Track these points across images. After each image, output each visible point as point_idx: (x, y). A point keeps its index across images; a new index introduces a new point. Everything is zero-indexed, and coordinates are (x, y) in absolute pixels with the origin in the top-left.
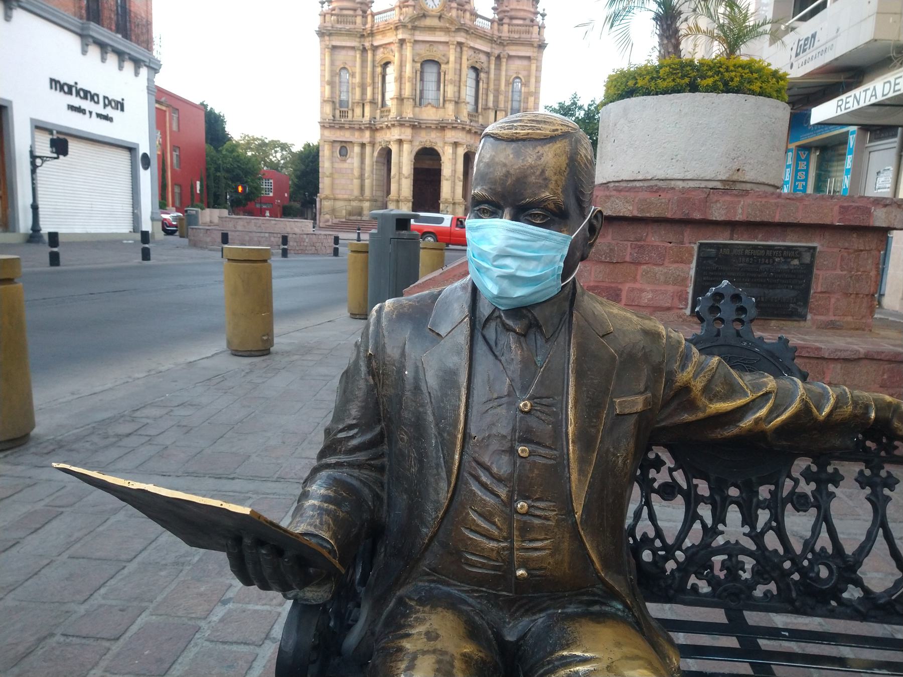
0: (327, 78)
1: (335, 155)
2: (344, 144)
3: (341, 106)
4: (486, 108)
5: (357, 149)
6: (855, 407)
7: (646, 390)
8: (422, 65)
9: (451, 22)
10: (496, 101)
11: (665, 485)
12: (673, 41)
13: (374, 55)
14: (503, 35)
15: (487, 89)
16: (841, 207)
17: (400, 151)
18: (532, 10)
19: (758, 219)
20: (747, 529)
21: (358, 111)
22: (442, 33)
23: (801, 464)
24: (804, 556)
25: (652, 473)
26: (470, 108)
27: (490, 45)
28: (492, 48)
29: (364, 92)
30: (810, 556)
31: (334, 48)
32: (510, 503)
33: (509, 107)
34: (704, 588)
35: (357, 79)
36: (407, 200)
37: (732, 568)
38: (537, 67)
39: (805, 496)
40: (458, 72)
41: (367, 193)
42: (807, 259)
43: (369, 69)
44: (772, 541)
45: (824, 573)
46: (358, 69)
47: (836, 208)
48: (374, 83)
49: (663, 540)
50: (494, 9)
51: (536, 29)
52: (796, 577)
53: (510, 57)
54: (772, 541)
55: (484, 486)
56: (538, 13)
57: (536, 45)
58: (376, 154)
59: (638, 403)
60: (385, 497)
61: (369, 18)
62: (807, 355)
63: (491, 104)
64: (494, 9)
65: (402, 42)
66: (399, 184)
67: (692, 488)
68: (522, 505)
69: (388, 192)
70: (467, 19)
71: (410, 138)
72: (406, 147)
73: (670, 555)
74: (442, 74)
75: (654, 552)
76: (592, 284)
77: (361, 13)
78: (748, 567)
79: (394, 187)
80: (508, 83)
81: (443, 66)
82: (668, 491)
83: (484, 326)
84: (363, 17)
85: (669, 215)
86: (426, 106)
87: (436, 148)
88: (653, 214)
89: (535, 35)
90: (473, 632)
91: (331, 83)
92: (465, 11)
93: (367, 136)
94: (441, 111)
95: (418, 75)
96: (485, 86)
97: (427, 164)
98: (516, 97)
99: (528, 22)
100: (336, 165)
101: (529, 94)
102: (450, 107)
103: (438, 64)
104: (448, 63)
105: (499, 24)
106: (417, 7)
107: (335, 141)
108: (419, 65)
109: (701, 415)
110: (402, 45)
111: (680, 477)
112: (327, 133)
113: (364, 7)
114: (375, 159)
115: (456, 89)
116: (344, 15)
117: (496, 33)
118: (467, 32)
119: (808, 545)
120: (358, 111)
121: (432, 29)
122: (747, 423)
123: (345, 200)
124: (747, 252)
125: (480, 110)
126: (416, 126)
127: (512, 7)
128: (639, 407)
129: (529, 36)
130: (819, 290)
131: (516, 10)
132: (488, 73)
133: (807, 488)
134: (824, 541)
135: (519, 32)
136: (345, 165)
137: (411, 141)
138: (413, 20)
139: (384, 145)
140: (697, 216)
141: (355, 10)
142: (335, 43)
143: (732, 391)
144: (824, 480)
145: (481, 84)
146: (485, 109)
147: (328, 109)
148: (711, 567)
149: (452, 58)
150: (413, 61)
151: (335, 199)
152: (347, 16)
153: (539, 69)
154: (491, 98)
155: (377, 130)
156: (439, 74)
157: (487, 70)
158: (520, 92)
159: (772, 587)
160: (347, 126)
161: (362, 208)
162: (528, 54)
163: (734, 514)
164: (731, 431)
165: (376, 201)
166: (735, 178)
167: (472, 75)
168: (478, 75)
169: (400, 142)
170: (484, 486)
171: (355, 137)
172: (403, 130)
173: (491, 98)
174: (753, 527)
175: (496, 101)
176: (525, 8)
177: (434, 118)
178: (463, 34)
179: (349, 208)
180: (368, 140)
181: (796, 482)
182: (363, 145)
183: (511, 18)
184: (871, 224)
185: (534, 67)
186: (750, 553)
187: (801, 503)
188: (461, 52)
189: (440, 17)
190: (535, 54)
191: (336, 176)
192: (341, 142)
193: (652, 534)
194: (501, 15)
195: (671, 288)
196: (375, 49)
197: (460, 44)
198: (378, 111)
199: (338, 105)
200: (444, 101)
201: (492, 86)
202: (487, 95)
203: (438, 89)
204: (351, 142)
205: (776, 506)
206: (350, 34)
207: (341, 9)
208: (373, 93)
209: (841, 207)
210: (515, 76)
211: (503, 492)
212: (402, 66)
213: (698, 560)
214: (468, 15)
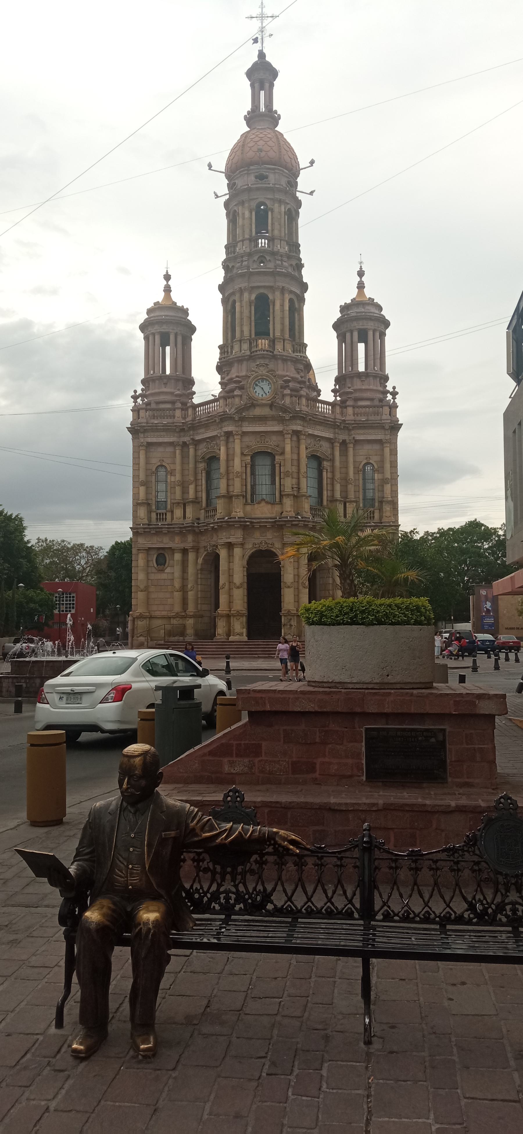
0: (142, 477)
1: (151, 564)
2: (161, 552)
3: (158, 508)
4: (333, 500)
6: (259, 833)
7: (177, 830)
8: (252, 457)
9: (284, 409)
10: (345, 491)
11: (205, 868)
12: (348, 581)
13: (196, 450)
14: (348, 418)
15: (333, 479)
16: (455, 701)
17: (230, 556)
18: (381, 389)
19: (399, 711)
20: (232, 884)
21: (178, 513)
22: (275, 423)
23: (255, 857)
24: (253, 893)
25: (201, 863)
26: (313, 501)
27: (332, 430)
28: (335, 433)
29: (185, 491)
30: (255, 892)
31: (149, 445)
32: (127, 866)
33: (361, 497)
34: (217, 907)
35: (178, 477)
36: (242, 615)
37: (227, 898)
38: (391, 450)
39: (253, 870)
40: (295, 463)
41: (191, 608)
42: (440, 738)
43: (191, 465)
44: (241, 888)
45: (259, 898)
46: (178, 467)
47: (452, 702)
48: (196, 480)
49: (203, 890)
50: (333, 391)
51: (386, 410)
52: (250, 901)
53: (356, 442)
54: (241, 888)
55: (120, 861)
56: (388, 392)
57: (387, 427)
58: (200, 561)
59: (173, 834)
60: (95, 871)
61: (190, 411)
62: (417, 809)
63: (338, 495)
64: (333, 391)
66: (230, 596)
67: (215, 868)
68: (130, 866)
69: (217, 606)
70: (303, 407)
71: (241, 540)
72: (237, 551)
73: (205, 895)
74: (277, 466)
75: (199, 894)
76: (294, 759)
77: (180, 405)
78: (233, 899)
79: (223, 599)
80: (357, 471)
81: (277, 457)
82: (206, 870)
83: (124, 811)
84: (182, 410)
85: (339, 710)
86: (259, 503)
88: (328, 709)
89: (385, 417)
90: (114, 903)
91: (146, 484)
92: (300, 397)
94: (277, 508)
95: (249, 466)
96: (330, 475)
98: (370, 486)
99: (376, 403)
100: (152, 577)
101: (384, 481)
102: (288, 503)
103: (271, 455)
104: (283, 453)
105: (341, 407)
106: (245, 397)
107: (150, 549)
108: (249, 458)
109: (200, 838)
111: (211, 866)
113: (184, 400)
114: (199, 567)
115: (294, 481)
116: (160, 410)
117: (338, 416)
118: (303, 419)
119: (255, 889)
120: (178, 513)
121: (262, 419)
122: (218, 841)
123: (163, 618)
124: (399, 733)
125: (325, 503)
126: (247, 526)
127: (355, 387)
128: (173, 835)
129: (379, 418)
130: (453, 759)
131: (361, 390)
132: (332, 460)
133: (255, 867)
134: (260, 887)
135: (366, 414)
136: (164, 576)
137: (242, 545)
138: (240, 410)
139: (210, 549)
140: (358, 710)
141: (173, 403)
142: (150, 440)
143: (212, 828)
144: (261, 863)
145: (324, 474)
146: (331, 501)
147: (142, 512)
148: (220, 899)
149: (288, 448)
150: (242, 454)
151: (151, 618)
152: (164, 410)
153: (394, 452)
154: (338, 487)
155: (201, 533)
156: (273, 466)
157: (330, 457)
158: (373, 479)
159: (242, 905)
160: (165, 531)
161: (184, 626)
162: (379, 437)
163: (228, 877)
164: (214, 844)
165: (202, 616)
166: (386, 681)
167: (314, 464)
168: (320, 465)
169: (230, 546)
170: (120, 861)
171: (177, 543)
172: (232, 532)
173: (338, 487)
174: (235, 882)
175: (345, 491)
176: (371, 387)
177: (269, 515)
178: (299, 422)
179: (168, 627)
180: (191, 545)
181: (252, 865)
183: (356, 400)
184: (478, 712)
185: (387, 451)
186: (233, 893)
187: (252, 872)
188: (299, 441)
189: (271, 406)
190: (388, 437)
191: (152, 589)
192: (159, 549)
193: (199, 888)
194: (344, 398)
195: (350, 761)
196: (196, 443)
197: (297, 433)
198: (203, 511)
199: (154, 507)
200: (281, 496)
201: (338, 475)
202: (333, 485)
203: (273, 482)
204: (171, 548)
205: (244, 874)
206: (167, 429)
207: (158, 403)
208: (196, 491)
209: (455, 701)
210: (365, 461)
211: (125, 864)
212: (229, 459)
213: (215, 897)
214: (304, 401)
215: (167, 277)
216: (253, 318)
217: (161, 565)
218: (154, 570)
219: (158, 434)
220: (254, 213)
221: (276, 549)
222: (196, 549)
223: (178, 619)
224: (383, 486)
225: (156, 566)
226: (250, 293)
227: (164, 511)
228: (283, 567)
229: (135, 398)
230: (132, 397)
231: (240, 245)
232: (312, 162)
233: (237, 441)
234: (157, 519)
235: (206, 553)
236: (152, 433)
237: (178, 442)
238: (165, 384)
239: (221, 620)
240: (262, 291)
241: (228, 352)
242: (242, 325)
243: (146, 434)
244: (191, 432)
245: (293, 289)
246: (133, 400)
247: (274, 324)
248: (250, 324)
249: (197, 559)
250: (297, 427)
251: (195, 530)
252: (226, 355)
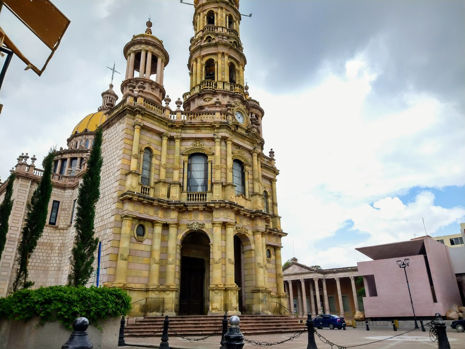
2: (142, 223)
5: (158, 229)
17: (224, 235)
35: (164, 161)
58: (180, 237)
65: (224, 139)
74: (246, 173)
81: (247, 168)
87: (247, 235)
93: (173, 216)
97: (194, 254)
112: (129, 208)
121: (242, 137)
123: (140, 290)
126: (238, 211)
136: (141, 247)
139: (195, 227)
142: (145, 123)
160: (156, 203)
171: (159, 216)
182: (166, 226)
196: (183, 139)
217: (140, 236)
218: (134, 240)
219: (153, 122)
220: (227, 17)
221: (249, 235)
222: (177, 225)
223: (156, 292)
224: (273, 207)
225: (136, 236)
227: (148, 187)
228: (254, 250)
231: (220, 30)
232: (250, 15)
234: (141, 192)
235: (188, 230)
237: (167, 134)
239: (219, 294)
240: (233, 61)
249: (177, 235)
251: (182, 209)
252: (211, 87)
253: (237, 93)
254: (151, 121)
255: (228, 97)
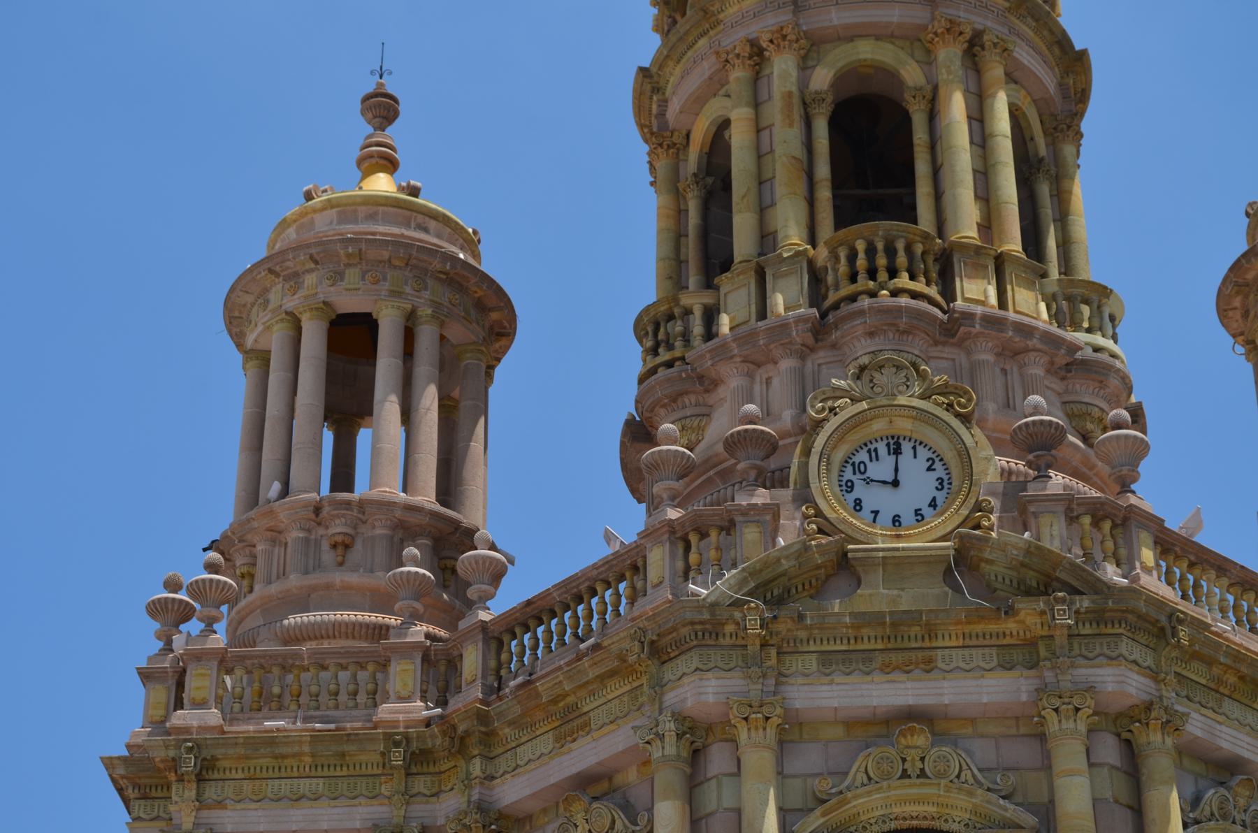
110: (696, 755)
215: (382, 108)
216: (823, 170)
219: (285, 786)
226: (805, 65)
229: (170, 615)
230: (156, 609)
233: (759, 760)
236: (247, 786)
238: (347, 547)
240: (866, 51)
241: (686, 337)
242: (763, 209)
243: (211, 792)
244: (476, 768)
245: (1024, 55)
246: (156, 626)
247: (938, 196)
248: (811, 202)
250: (1120, 681)
253: (853, 298)
254: (271, 787)
255: (786, 364)
